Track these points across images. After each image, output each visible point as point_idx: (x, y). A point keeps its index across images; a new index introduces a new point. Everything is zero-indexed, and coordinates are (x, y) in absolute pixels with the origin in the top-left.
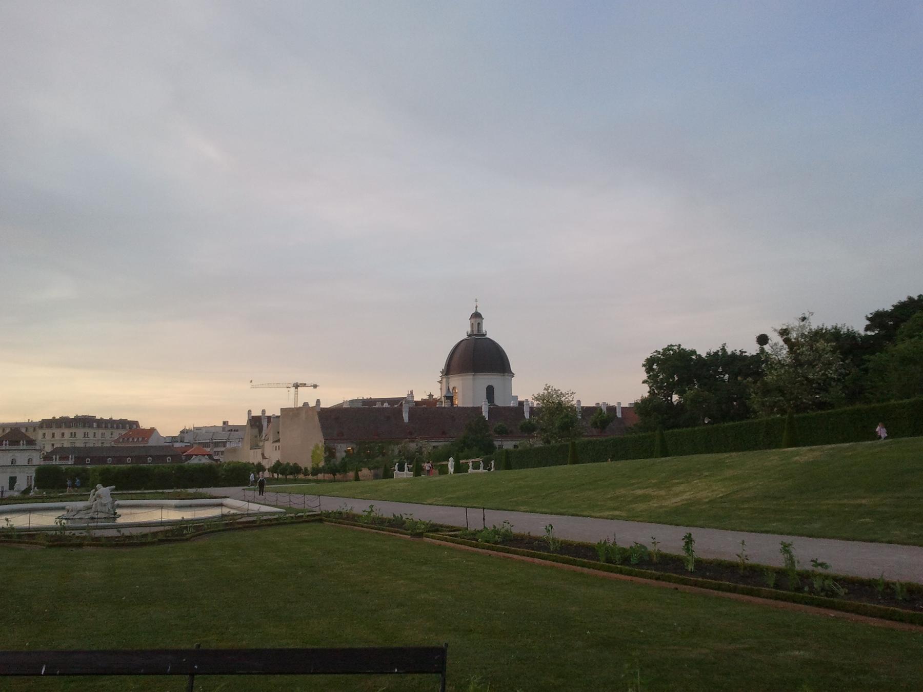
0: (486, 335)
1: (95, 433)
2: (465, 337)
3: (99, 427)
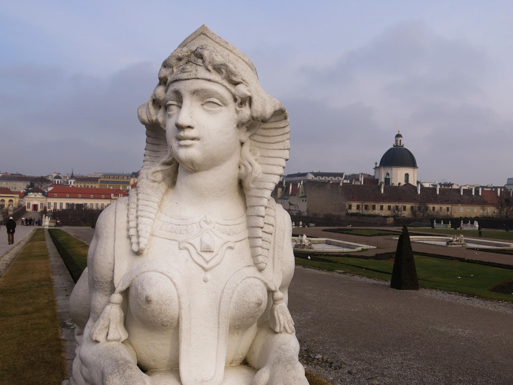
2: (392, 147)
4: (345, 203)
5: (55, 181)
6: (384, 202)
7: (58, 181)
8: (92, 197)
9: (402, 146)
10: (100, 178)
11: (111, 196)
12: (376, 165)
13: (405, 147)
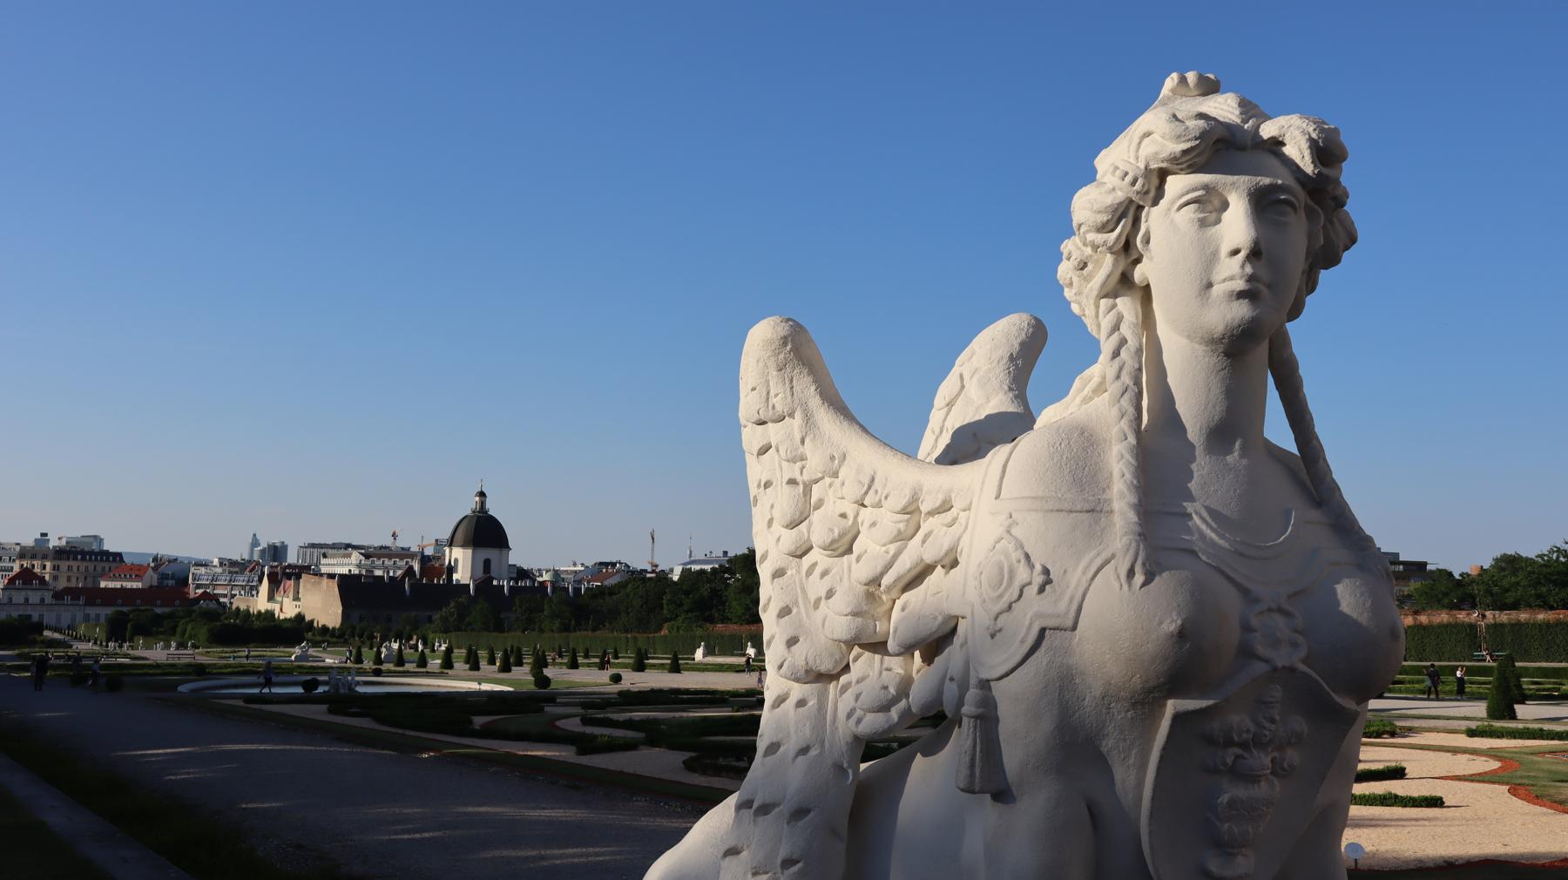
3: (83, 559)
13: (490, 513)
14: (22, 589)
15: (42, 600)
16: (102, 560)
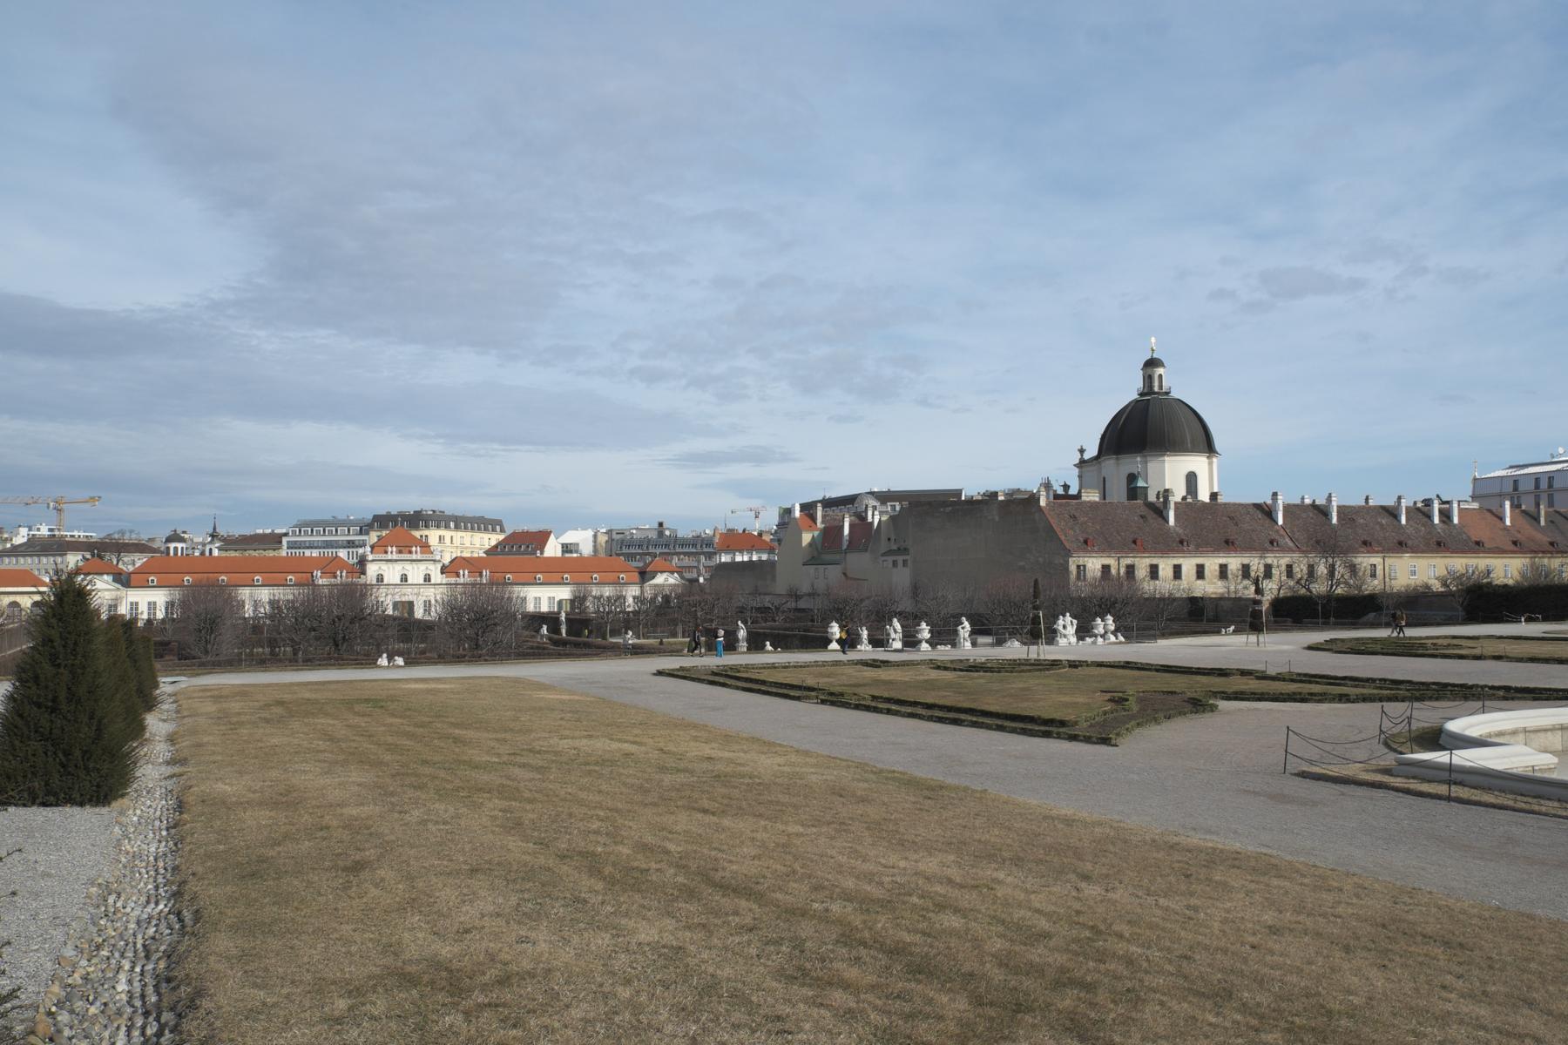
0: (1169, 393)
1: (452, 537)
2: (1134, 396)
3: (457, 527)
4: (1062, 561)
5: (168, 548)
6: (1183, 552)
7: (176, 549)
8: (260, 583)
9: (1167, 393)
10: (286, 535)
11: (313, 576)
12: (1082, 455)
14: (396, 561)
15: (427, 578)
16: (479, 529)
